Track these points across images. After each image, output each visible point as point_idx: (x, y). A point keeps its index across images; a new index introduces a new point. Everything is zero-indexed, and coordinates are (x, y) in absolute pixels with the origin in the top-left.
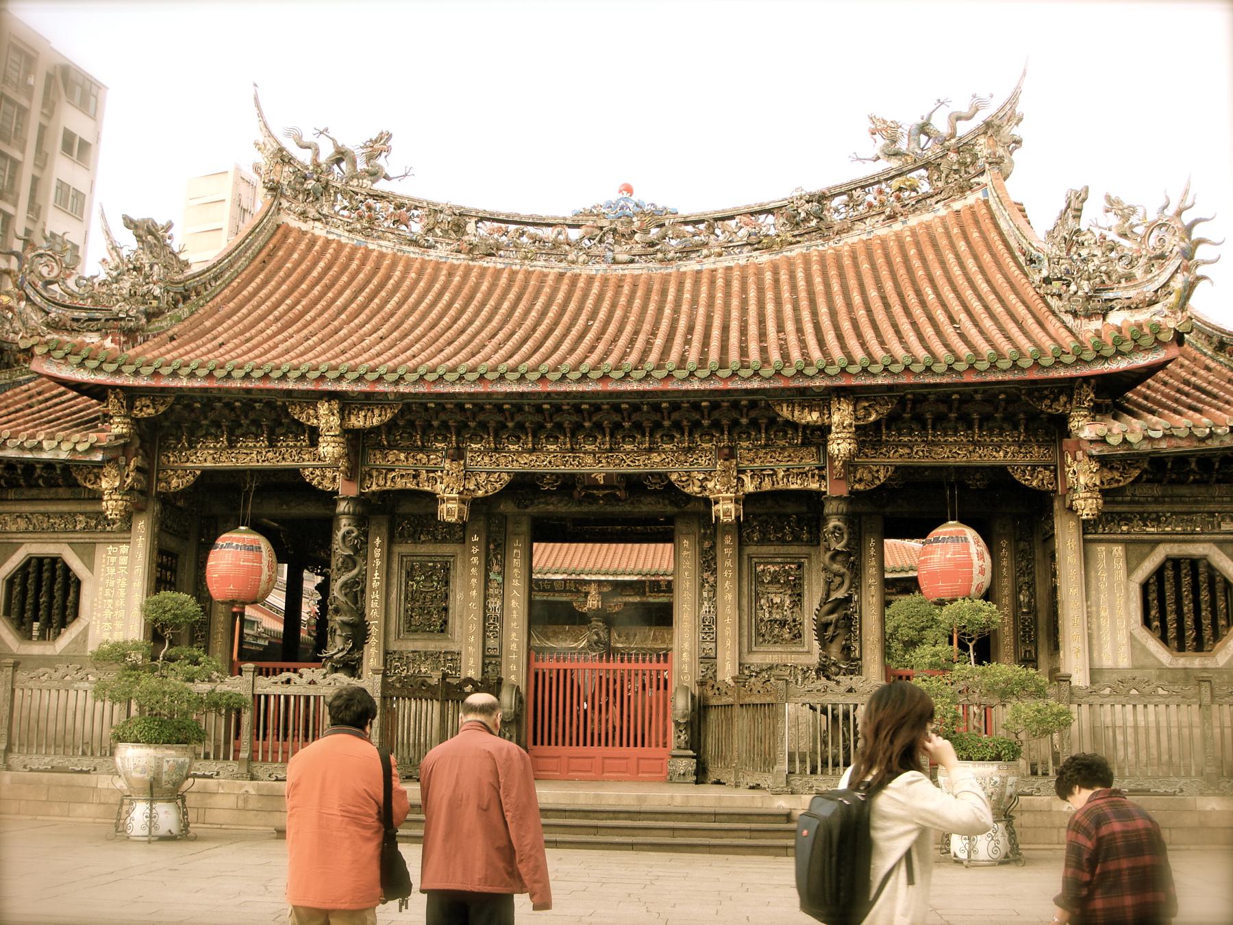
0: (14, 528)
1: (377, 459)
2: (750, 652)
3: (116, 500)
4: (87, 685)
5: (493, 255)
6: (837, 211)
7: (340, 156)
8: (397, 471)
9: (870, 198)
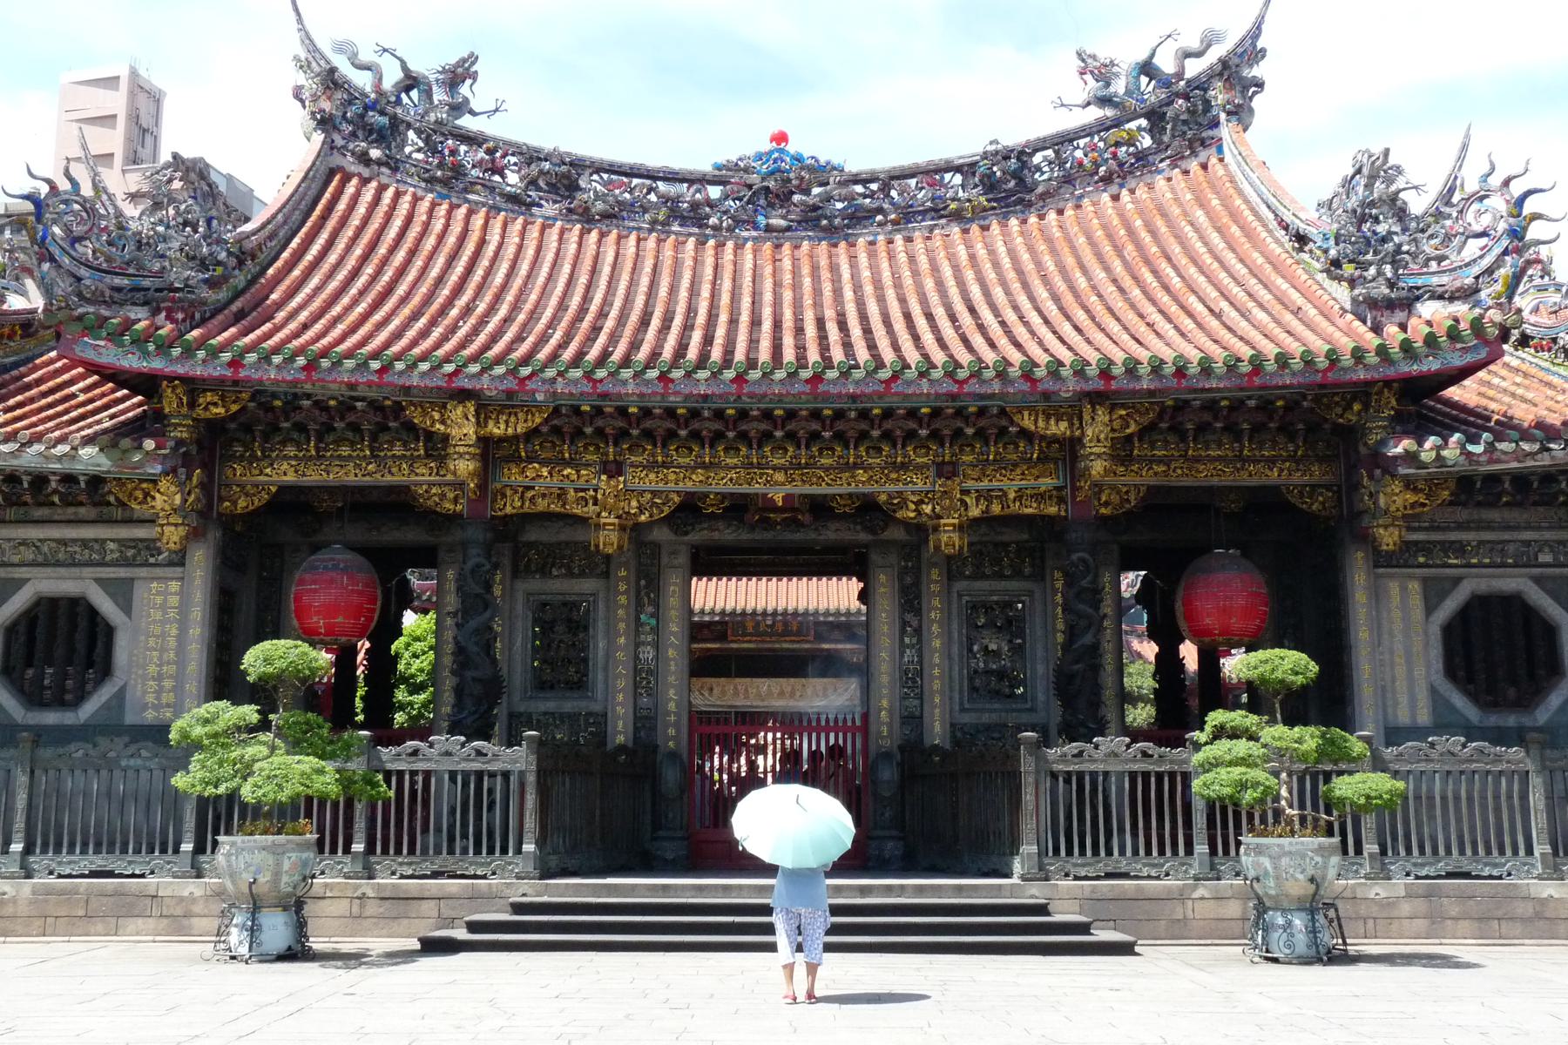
0: (16, 559)
1: (513, 476)
2: (963, 710)
3: (176, 525)
4: (139, 762)
5: (614, 216)
6: (1038, 169)
8: (535, 484)
9: (1079, 154)
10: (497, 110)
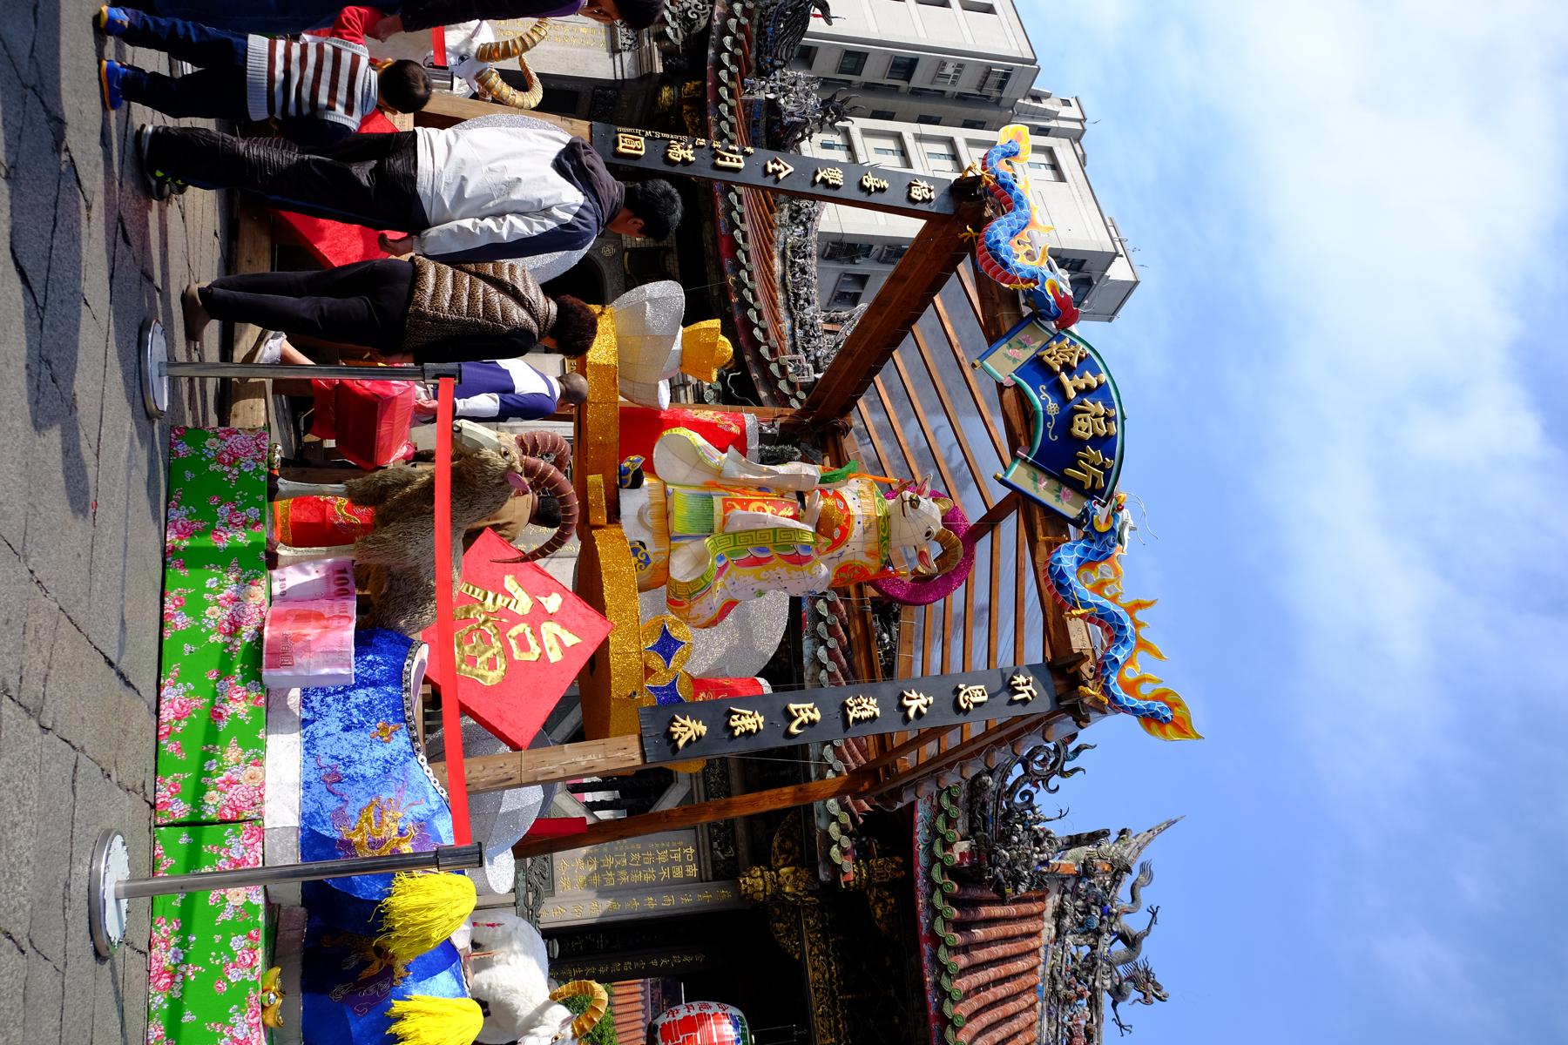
7: (1132, 942)
10: (1121, 1027)
